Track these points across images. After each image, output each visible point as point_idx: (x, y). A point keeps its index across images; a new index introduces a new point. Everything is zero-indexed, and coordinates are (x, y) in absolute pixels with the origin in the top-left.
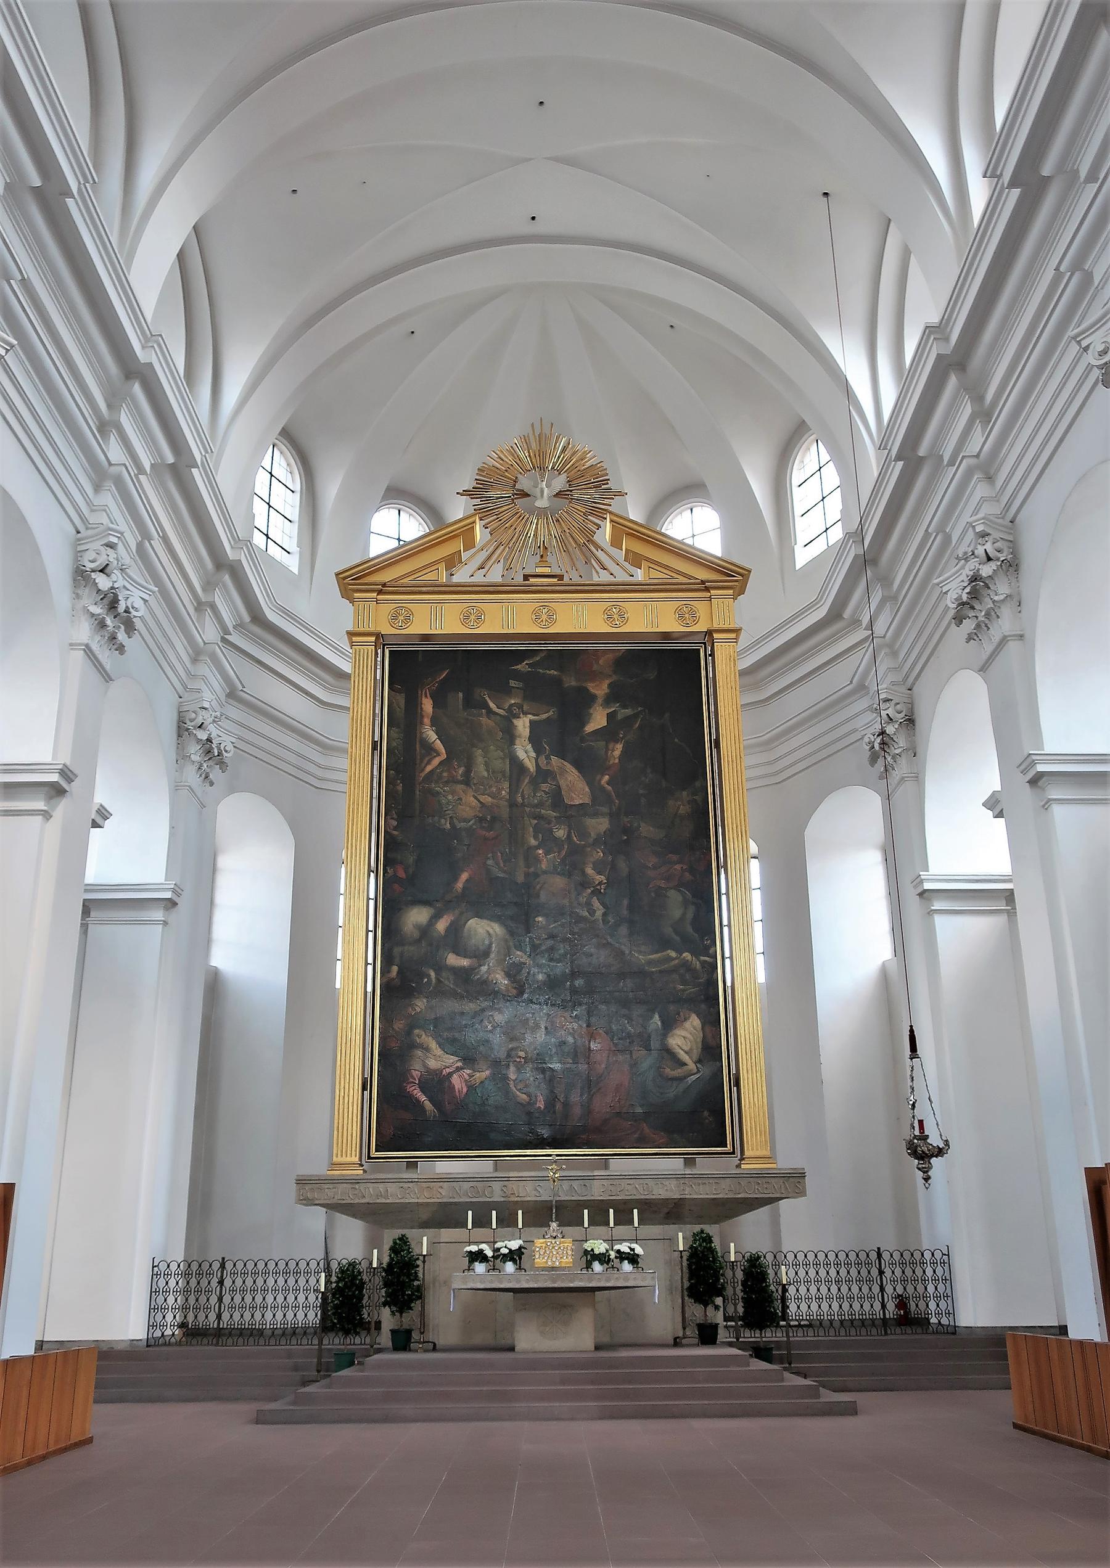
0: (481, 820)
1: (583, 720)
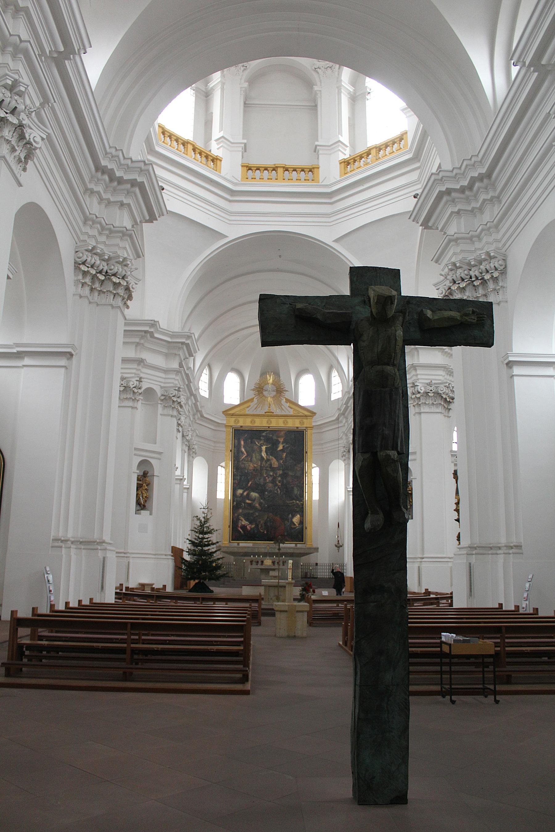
0: (254, 470)
1: (277, 448)
